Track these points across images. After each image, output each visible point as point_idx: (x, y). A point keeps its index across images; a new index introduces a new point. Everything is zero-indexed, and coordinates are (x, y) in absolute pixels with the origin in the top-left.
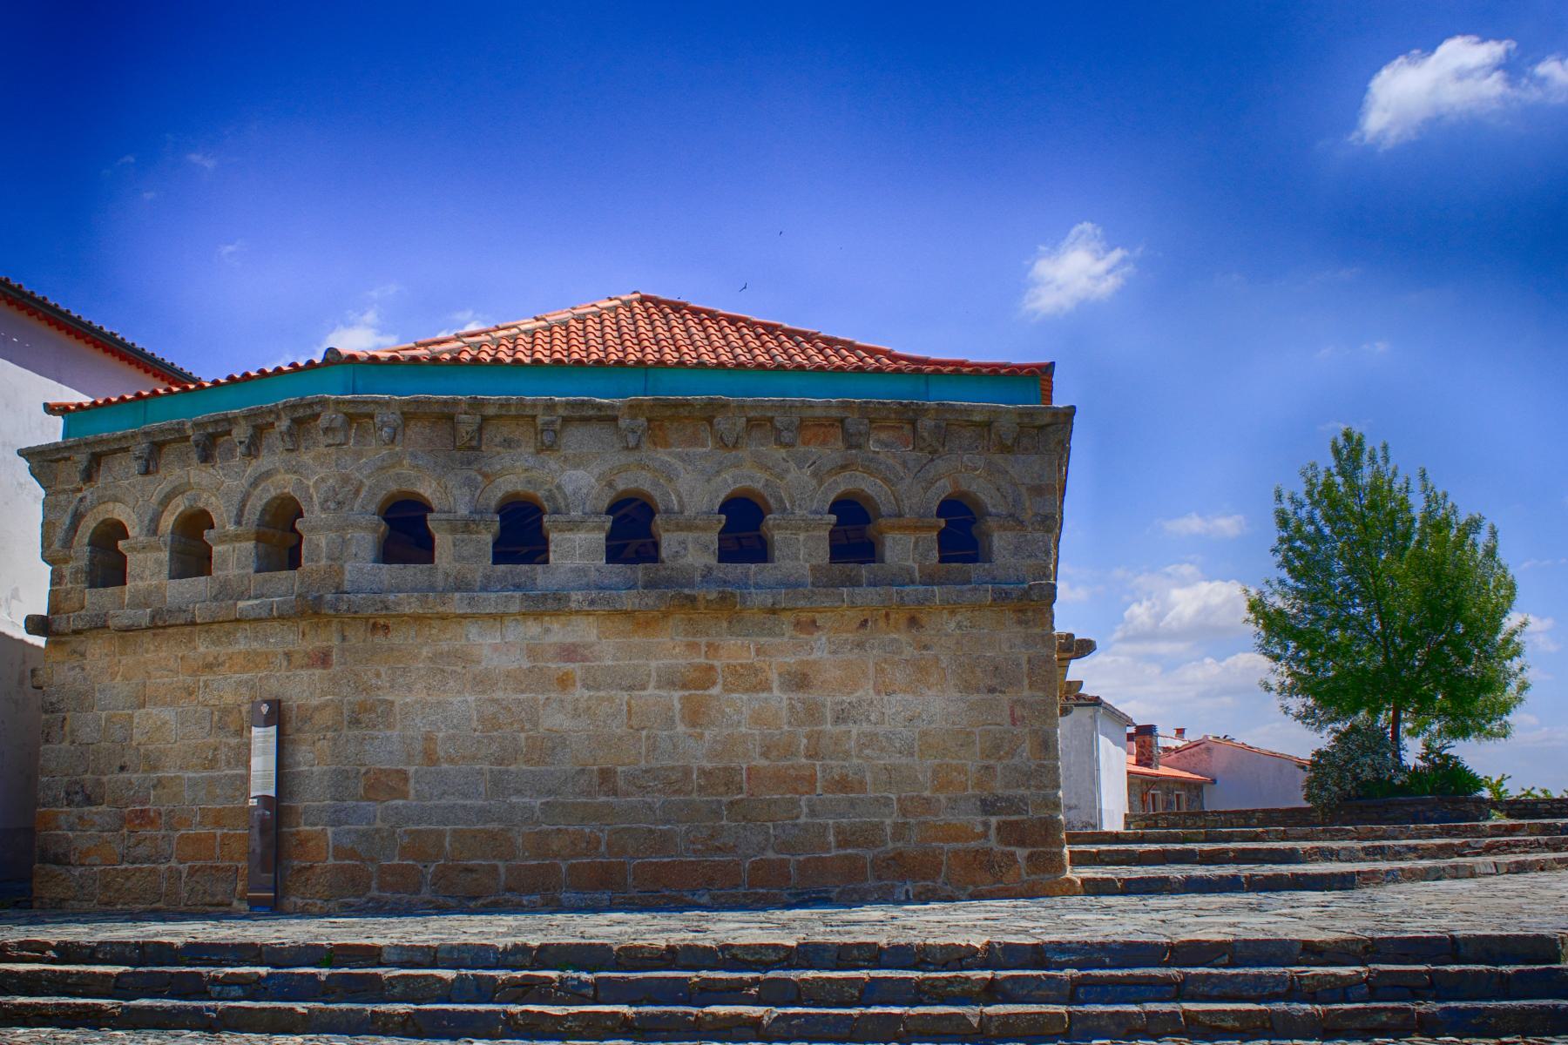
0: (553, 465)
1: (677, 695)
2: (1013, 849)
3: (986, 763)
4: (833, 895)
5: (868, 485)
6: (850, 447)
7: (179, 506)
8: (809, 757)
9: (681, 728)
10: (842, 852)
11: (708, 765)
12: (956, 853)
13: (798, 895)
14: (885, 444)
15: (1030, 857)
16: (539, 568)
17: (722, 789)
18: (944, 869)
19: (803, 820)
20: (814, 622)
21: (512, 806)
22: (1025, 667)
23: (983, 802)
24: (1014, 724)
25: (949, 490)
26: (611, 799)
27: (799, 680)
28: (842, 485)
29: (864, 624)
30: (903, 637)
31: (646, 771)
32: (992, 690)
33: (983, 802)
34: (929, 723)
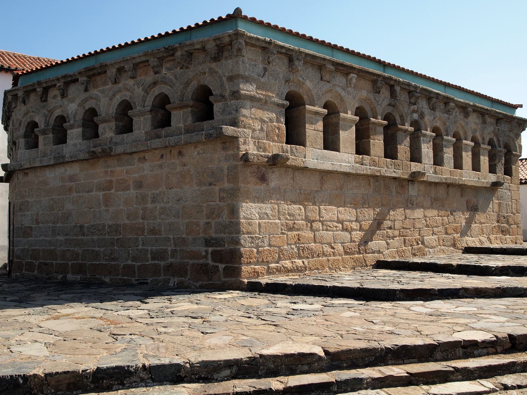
0: (66, 103)
1: (102, 193)
2: (217, 264)
3: (208, 221)
4: (149, 281)
5: (165, 89)
6: (155, 73)
8: (142, 219)
9: (103, 208)
10: (153, 262)
11: (110, 223)
12: (193, 265)
13: (137, 280)
14: (169, 69)
15: (224, 269)
16: (64, 145)
17: (115, 233)
18: (189, 272)
19: (140, 247)
20: (144, 158)
21: (57, 240)
22: (226, 172)
23: (206, 240)
24: (220, 201)
25: (196, 86)
26: (83, 237)
28: (156, 91)
29: (162, 156)
30: (177, 162)
31: (92, 226)
32: (210, 184)
33: (206, 240)
34: (185, 202)
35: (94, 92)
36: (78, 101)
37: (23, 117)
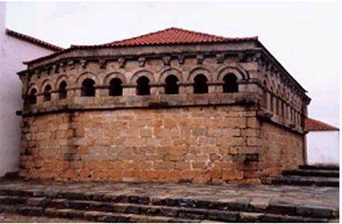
7: (46, 84)
27: (184, 124)
35: (147, 67)
36: (135, 71)
37: (81, 75)
